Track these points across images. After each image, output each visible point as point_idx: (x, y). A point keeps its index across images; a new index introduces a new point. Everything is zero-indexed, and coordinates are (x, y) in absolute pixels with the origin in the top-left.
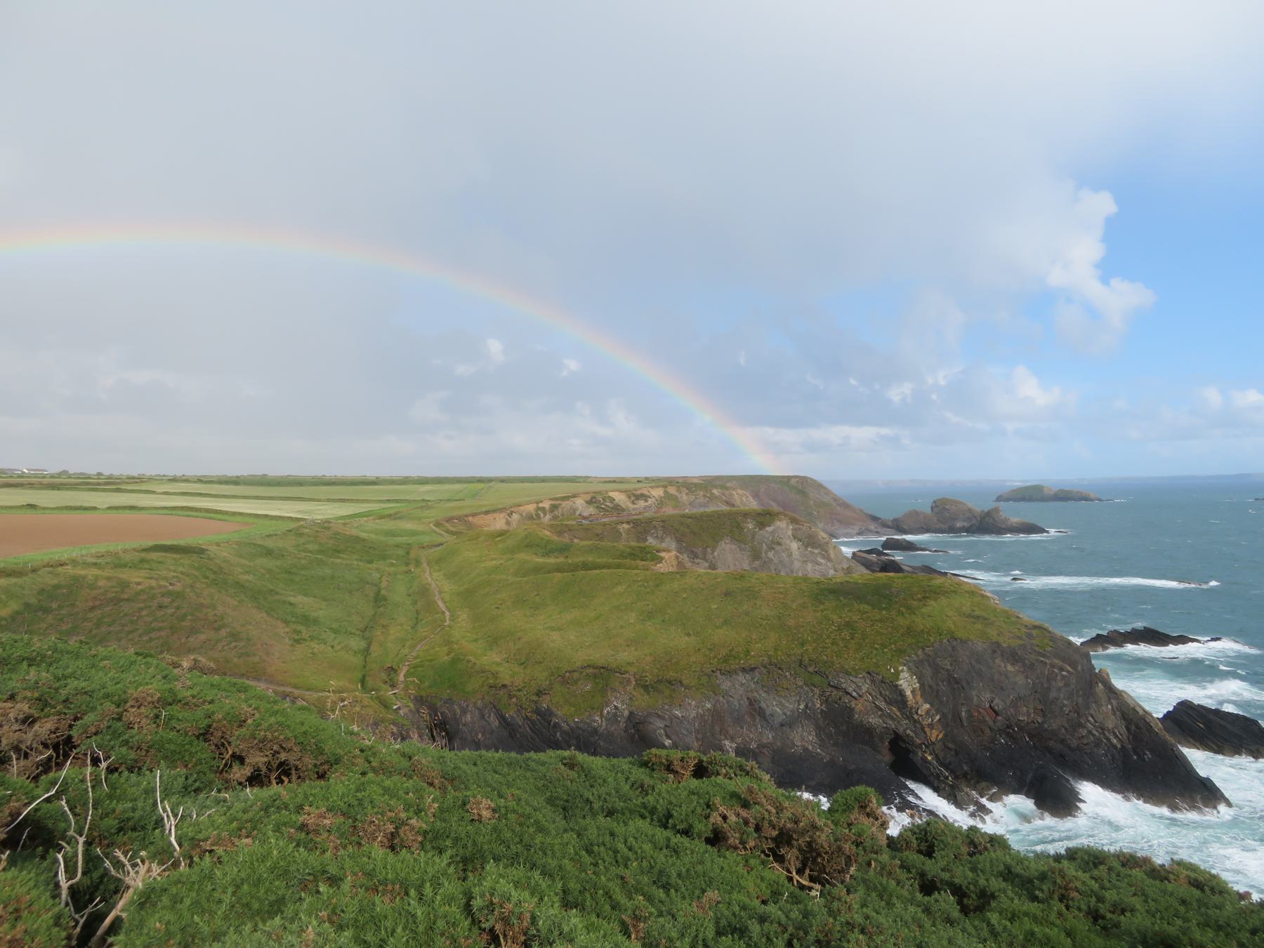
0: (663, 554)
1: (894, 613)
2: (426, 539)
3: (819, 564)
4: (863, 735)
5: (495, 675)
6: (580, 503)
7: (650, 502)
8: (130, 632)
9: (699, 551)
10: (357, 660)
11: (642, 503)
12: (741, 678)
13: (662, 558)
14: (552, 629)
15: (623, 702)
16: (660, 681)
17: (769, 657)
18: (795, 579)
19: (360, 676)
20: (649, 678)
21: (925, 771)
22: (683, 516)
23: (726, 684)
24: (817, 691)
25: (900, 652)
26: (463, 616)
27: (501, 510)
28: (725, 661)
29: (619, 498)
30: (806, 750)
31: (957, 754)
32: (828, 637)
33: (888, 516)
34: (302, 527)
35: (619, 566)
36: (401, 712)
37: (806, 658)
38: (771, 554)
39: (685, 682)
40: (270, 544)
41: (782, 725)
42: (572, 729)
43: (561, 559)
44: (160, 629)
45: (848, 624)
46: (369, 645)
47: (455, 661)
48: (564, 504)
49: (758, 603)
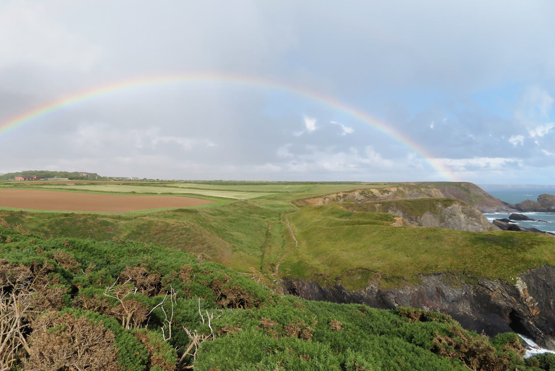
0: (396, 218)
1: (515, 251)
2: (288, 209)
3: (474, 225)
4: (496, 309)
5: (317, 270)
6: (357, 194)
7: (390, 194)
8: (170, 244)
9: (414, 217)
10: (259, 260)
11: (386, 194)
12: (433, 278)
13: (396, 220)
14: (343, 251)
15: (375, 285)
16: (393, 277)
17: (448, 269)
18: (462, 232)
19: (260, 266)
20: (388, 275)
21: (528, 329)
22: (406, 201)
23: (425, 280)
24: (472, 286)
25: (517, 270)
26: (304, 243)
27: (320, 197)
28: (425, 270)
29: (375, 192)
30: (465, 314)
31: (547, 322)
32: (479, 261)
33: (514, 203)
34: (236, 202)
35: (375, 223)
36: (277, 283)
37: (467, 270)
38: (450, 220)
39: (406, 278)
40: (223, 209)
41: (453, 301)
42: (351, 295)
43: (348, 219)
44: (181, 243)
45: (489, 255)
46: (264, 254)
47: (300, 262)
48: (349, 194)
49: (443, 243)
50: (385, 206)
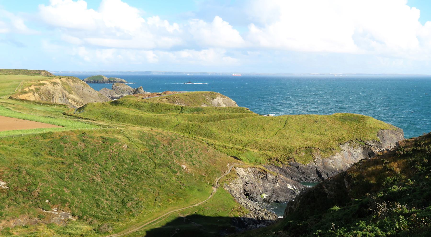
50: (171, 101)
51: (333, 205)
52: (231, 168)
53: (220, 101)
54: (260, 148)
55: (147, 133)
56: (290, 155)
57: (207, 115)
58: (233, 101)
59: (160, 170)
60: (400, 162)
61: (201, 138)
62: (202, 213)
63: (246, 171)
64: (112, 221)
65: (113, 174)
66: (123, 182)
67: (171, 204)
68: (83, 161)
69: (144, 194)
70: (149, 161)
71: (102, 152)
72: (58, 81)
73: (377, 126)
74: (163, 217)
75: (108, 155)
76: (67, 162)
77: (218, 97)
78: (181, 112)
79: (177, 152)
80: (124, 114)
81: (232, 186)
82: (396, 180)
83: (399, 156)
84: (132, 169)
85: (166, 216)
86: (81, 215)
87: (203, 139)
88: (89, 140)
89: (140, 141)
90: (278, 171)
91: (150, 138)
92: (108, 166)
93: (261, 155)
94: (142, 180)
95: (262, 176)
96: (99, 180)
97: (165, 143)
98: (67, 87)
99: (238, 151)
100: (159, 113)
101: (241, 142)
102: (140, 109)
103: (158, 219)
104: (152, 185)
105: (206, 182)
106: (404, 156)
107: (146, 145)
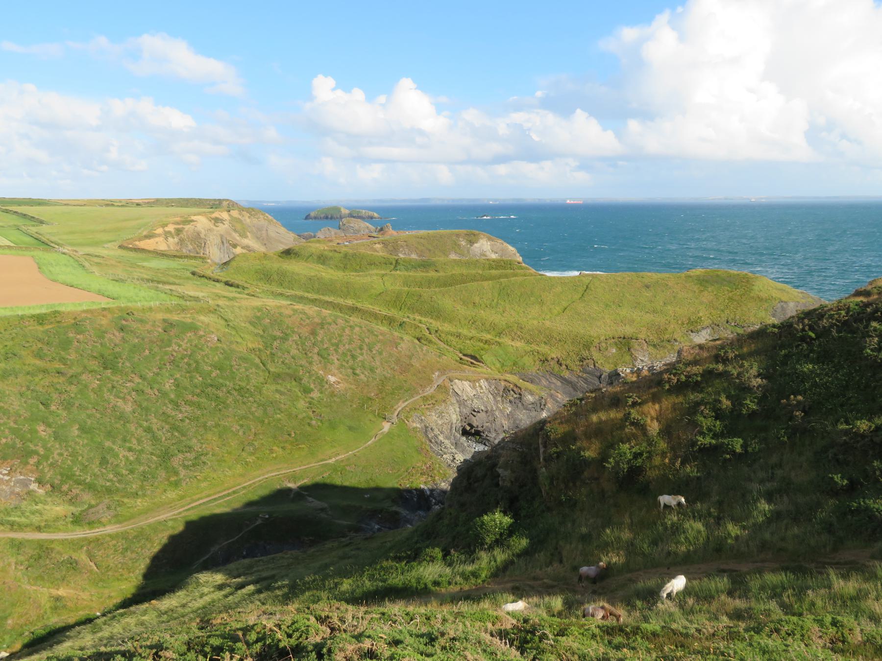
11: (222, 228)
51: (488, 509)
52: (440, 382)
53: (486, 247)
54: (529, 338)
55: (272, 312)
56: (585, 354)
57: (441, 274)
58: (511, 248)
59: (273, 387)
60: (667, 402)
61: (418, 317)
62: (338, 481)
63: (474, 387)
64: (123, 497)
65: (165, 394)
66: (181, 412)
67: (275, 458)
68: (105, 368)
69: (220, 437)
70: (257, 367)
71: (156, 349)
72: (225, 215)
73: (774, 295)
74: (244, 488)
75: (166, 357)
76: (71, 372)
77: (481, 241)
78: (395, 269)
79: (327, 349)
80: (293, 273)
81: (433, 418)
82: (641, 454)
83: (667, 387)
84: (211, 386)
85: (250, 485)
86: (57, 482)
87: (423, 319)
88: (134, 325)
89: (251, 328)
90: (559, 384)
91: (275, 321)
92: (159, 378)
93: (526, 353)
94: (227, 407)
95: (512, 396)
96: (128, 408)
97: (305, 332)
98: (238, 226)
99: (482, 344)
100: (356, 271)
101: (493, 327)
102: (323, 263)
103: (230, 491)
104: (247, 418)
105: (373, 412)
106: (681, 388)
107: (262, 336)
